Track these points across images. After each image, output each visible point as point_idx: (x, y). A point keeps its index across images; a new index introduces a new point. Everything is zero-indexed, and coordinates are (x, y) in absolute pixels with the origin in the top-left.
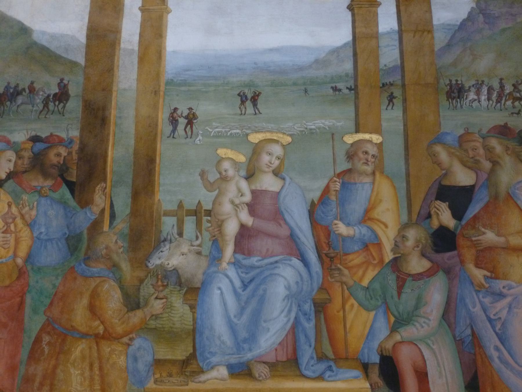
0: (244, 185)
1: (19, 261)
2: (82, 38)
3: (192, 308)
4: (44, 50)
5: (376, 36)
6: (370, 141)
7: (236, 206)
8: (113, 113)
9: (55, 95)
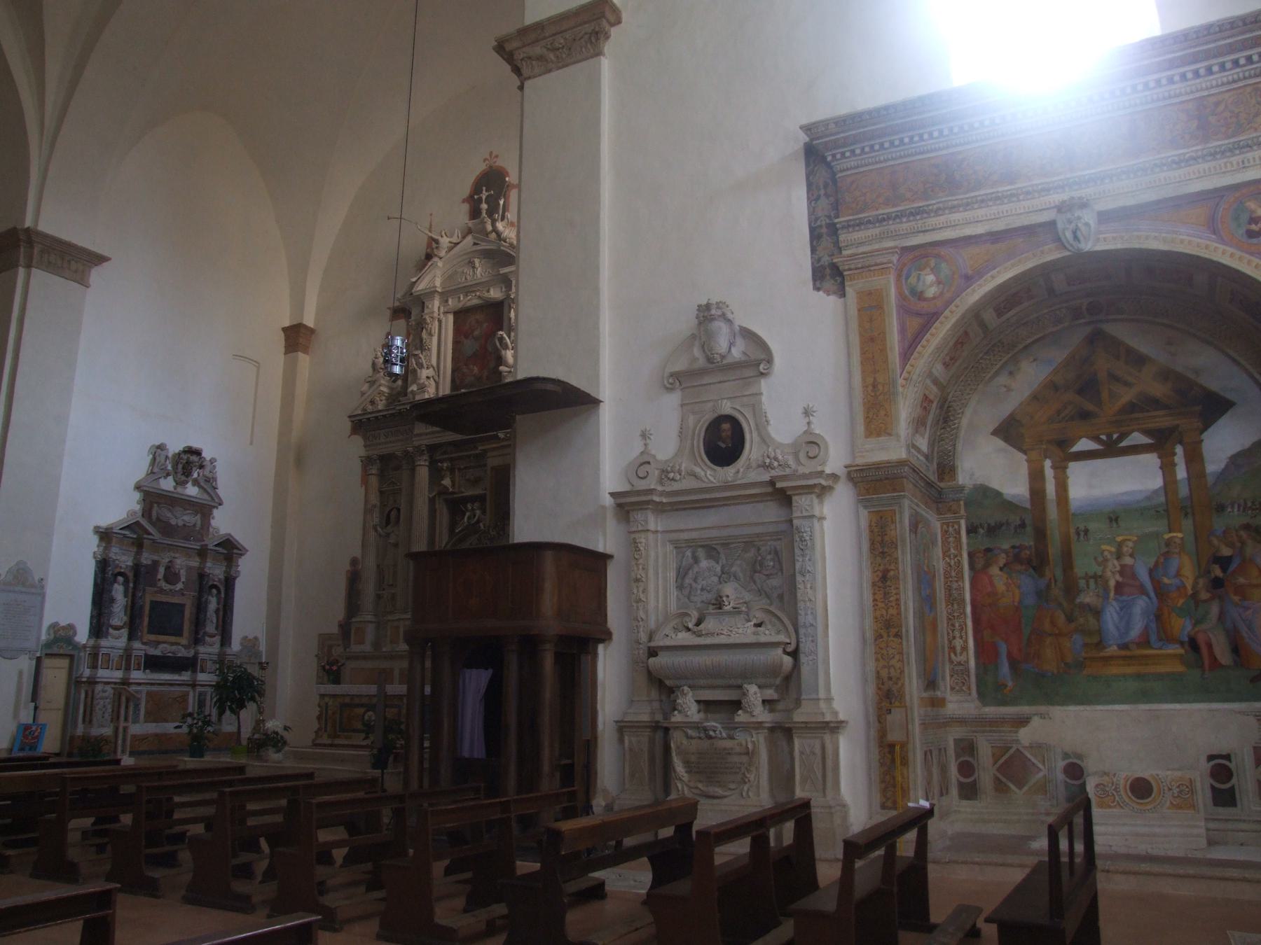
0: (1116, 562)
1: (1016, 604)
2: (1028, 496)
3: (1098, 620)
4: (1010, 503)
5: (1175, 482)
6: (1176, 537)
7: (1113, 573)
8: (1048, 532)
9: (1019, 525)
